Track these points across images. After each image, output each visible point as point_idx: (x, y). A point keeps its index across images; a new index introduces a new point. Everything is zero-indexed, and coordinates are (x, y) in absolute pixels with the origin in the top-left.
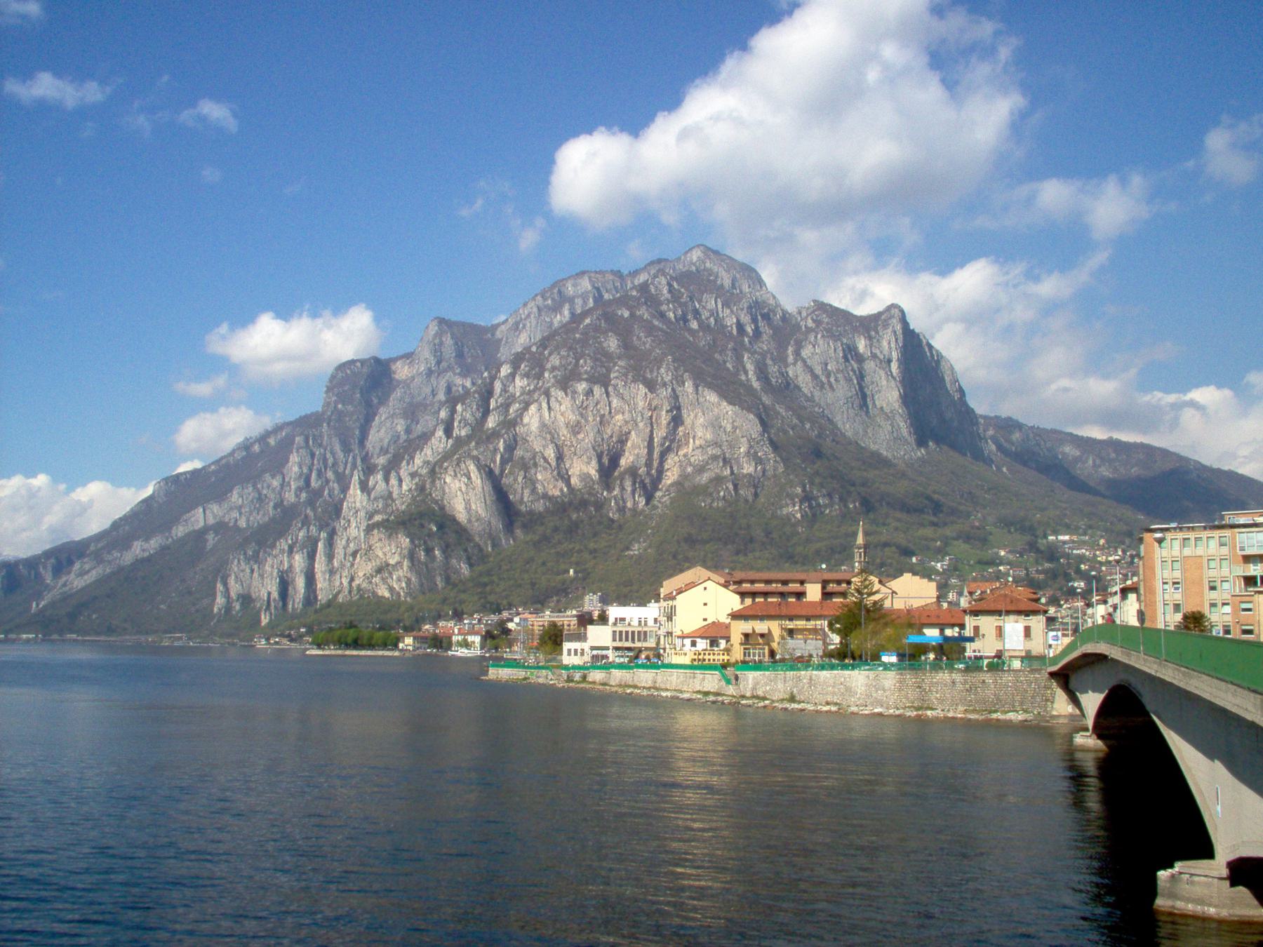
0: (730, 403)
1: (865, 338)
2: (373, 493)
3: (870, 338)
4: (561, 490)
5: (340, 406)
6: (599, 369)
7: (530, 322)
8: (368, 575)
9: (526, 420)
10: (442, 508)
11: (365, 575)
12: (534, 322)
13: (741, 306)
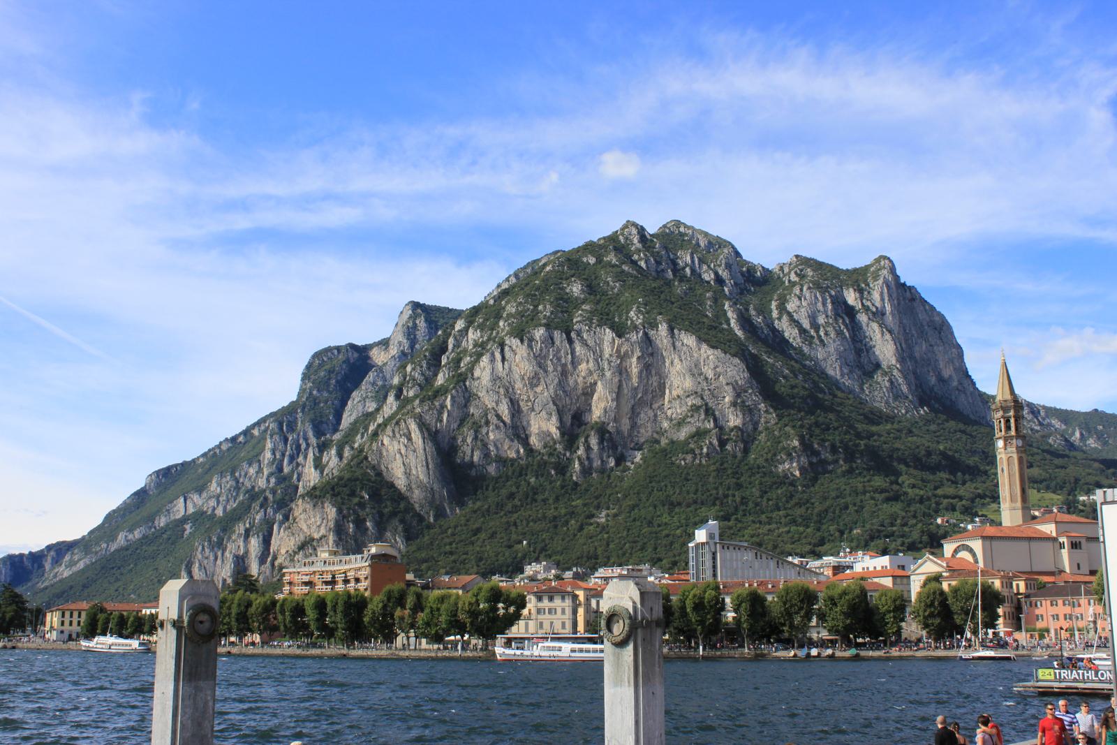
0: (713, 347)
1: (855, 290)
2: (326, 469)
3: (861, 291)
4: (518, 452)
5: (315, 392)
6: (560, 315)
8: (290, 552)
9: (477, 373)
10: (379, 474)
11: (287, 551)
13: (718, 263)
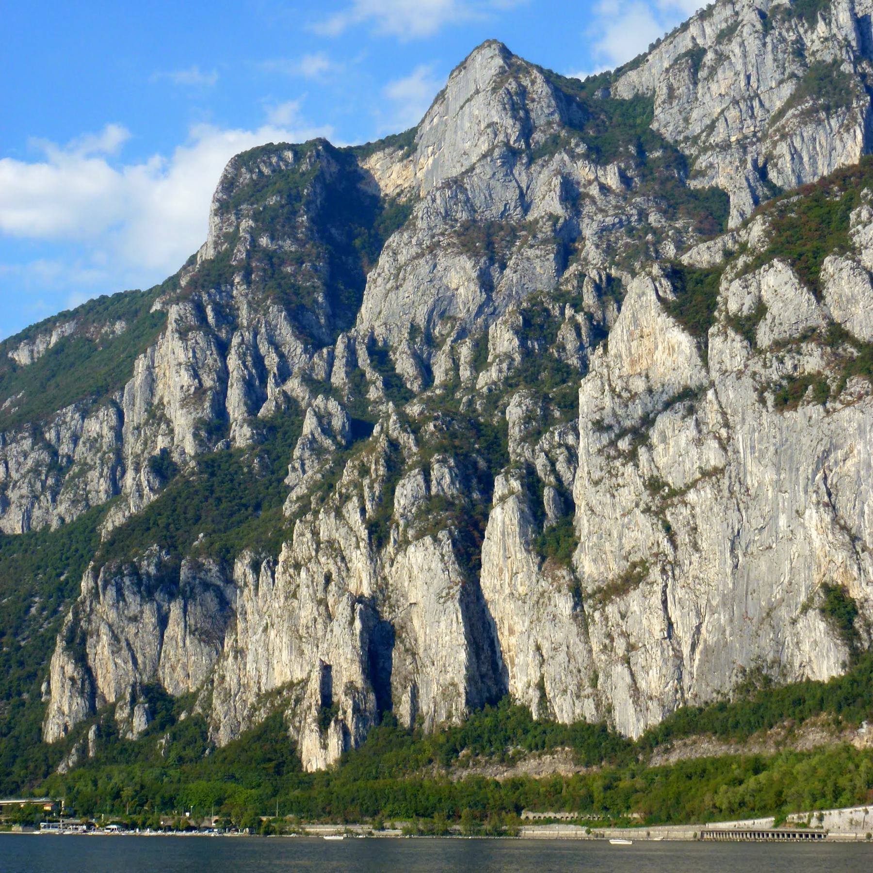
5: (264, 241)
7: (742, 44)
12: (753, 44)
